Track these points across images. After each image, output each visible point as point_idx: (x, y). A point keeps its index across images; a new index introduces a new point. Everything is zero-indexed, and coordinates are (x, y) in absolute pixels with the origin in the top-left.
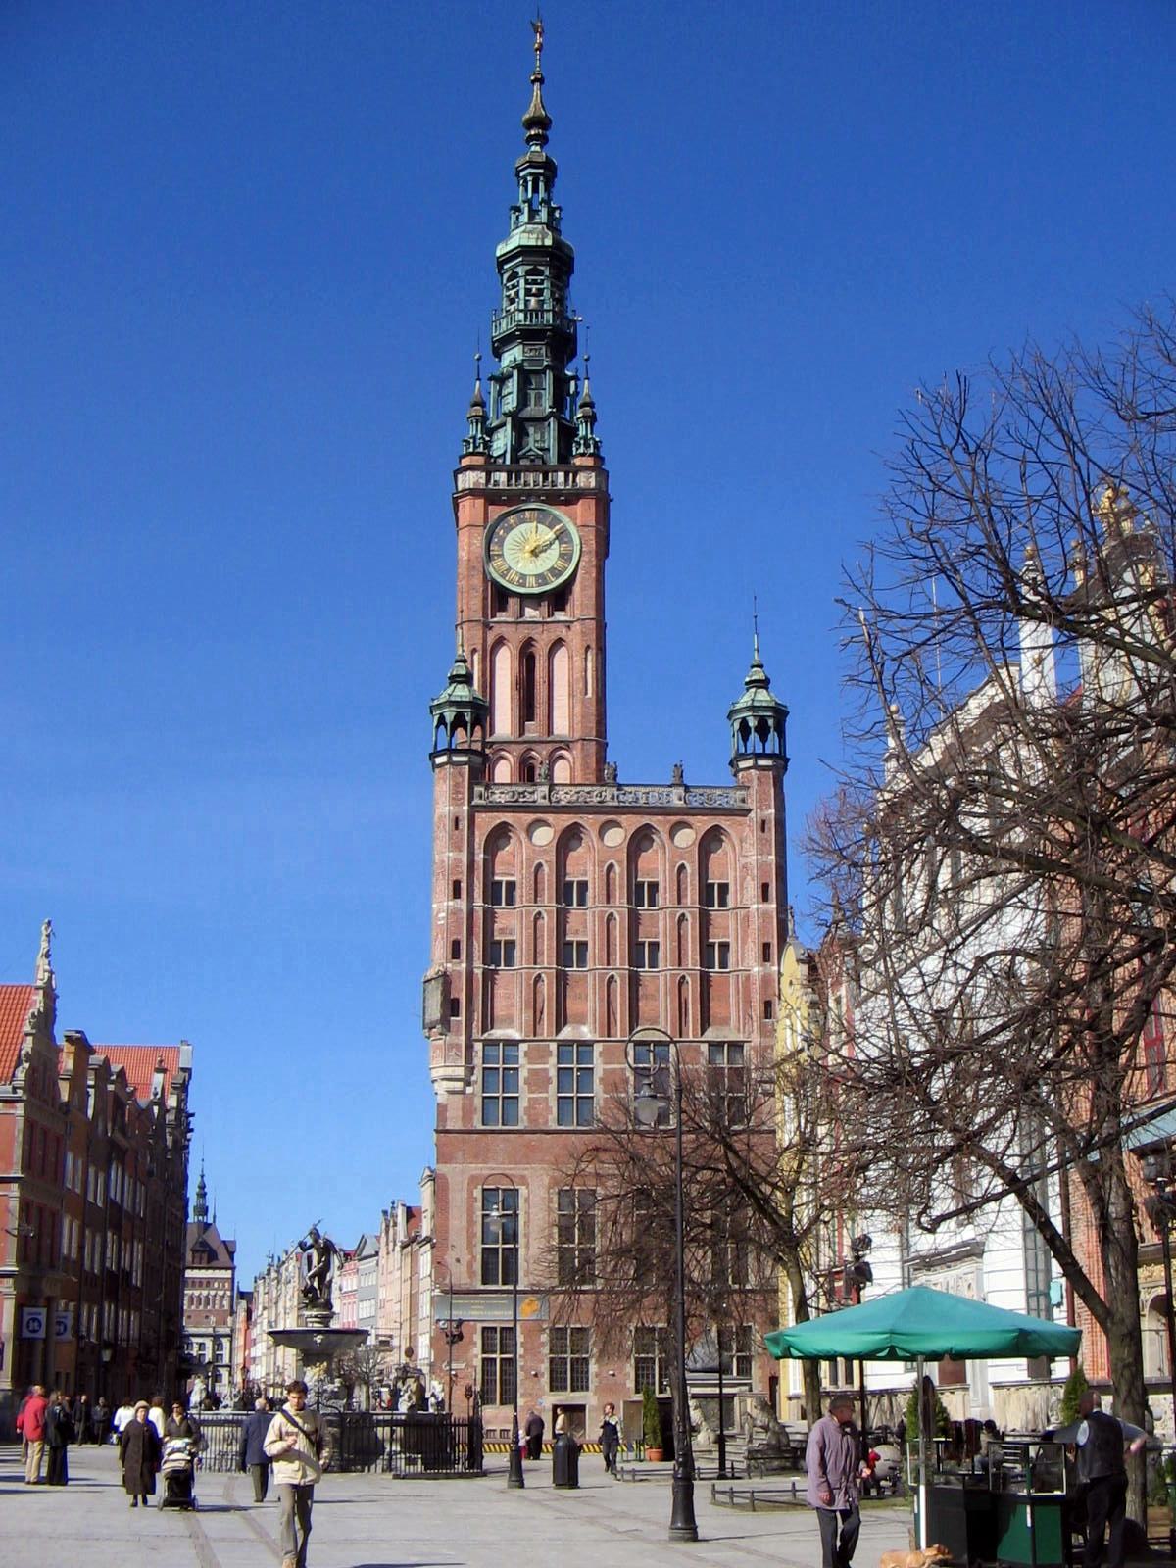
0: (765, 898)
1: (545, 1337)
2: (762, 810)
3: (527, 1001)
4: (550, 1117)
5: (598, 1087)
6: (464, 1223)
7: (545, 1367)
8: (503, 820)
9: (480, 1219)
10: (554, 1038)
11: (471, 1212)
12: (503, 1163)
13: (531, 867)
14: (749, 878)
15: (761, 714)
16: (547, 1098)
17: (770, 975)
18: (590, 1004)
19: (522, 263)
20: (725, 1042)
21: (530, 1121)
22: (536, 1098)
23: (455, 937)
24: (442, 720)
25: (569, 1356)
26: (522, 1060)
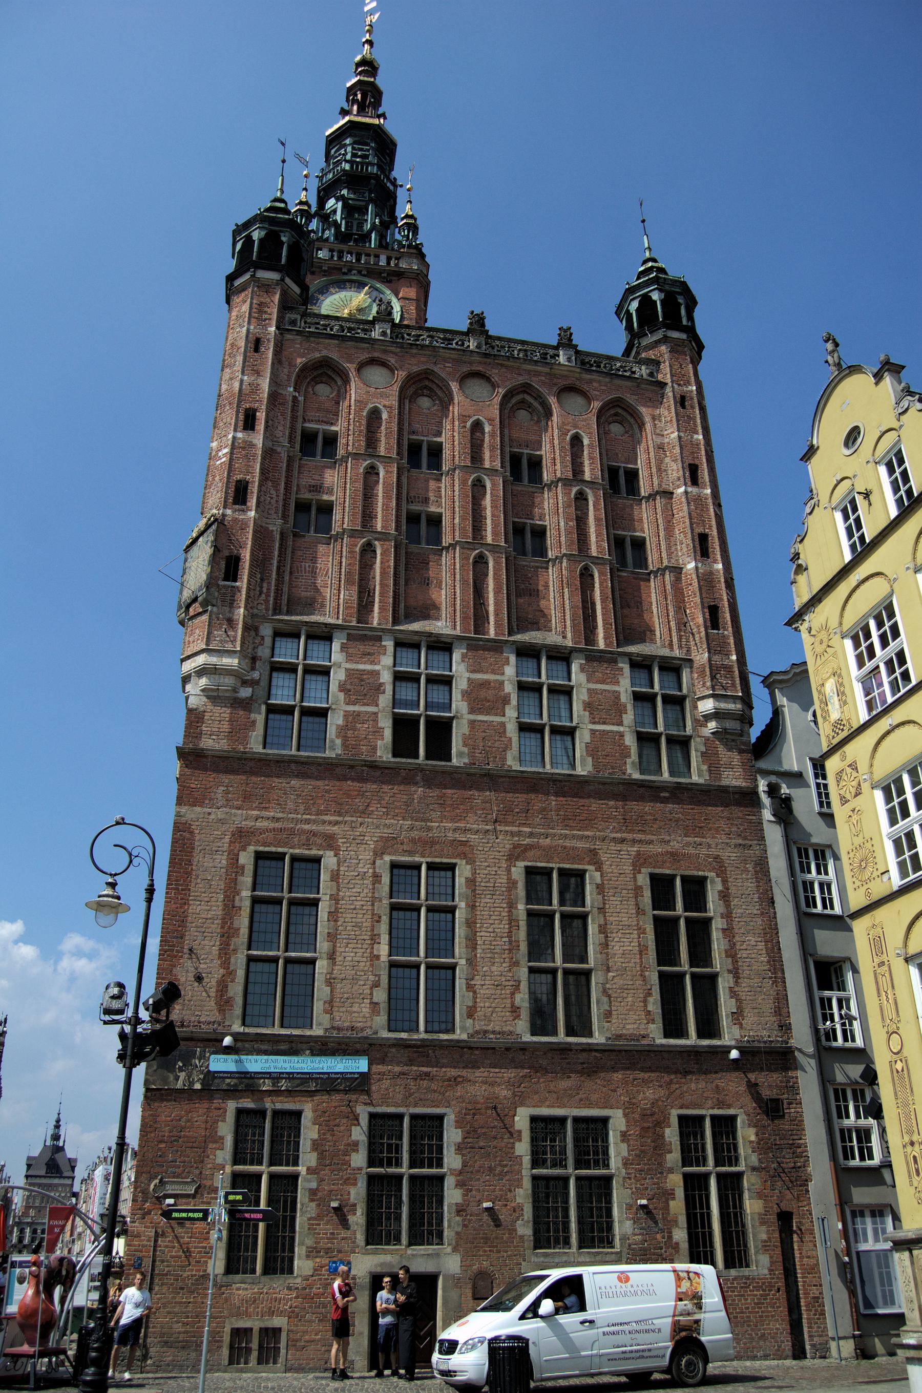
0: (695, 481)
1: (359, 1134)
2: (679, 385)
3: (348, 574)
4: (379, 743)
5: (459, 705)
6: (217, 910)
7: (357, 1193)
8: (325, 353)
9: (247, 904)
10: (389, 626)
11: (231, 890)
12: (296, 812)
13: (361, 410)
14: (667, 460)
15: (667, 287)
16: (376, 714)
17: (711, 573)
18: (443, 592)
19: (350, 136)
20: (653, 658)
21: (345, 745)
22: (359, 714)
23: (239, 477)
24: (249, 240)
25: (404, 1169)
26: (337, 655)
